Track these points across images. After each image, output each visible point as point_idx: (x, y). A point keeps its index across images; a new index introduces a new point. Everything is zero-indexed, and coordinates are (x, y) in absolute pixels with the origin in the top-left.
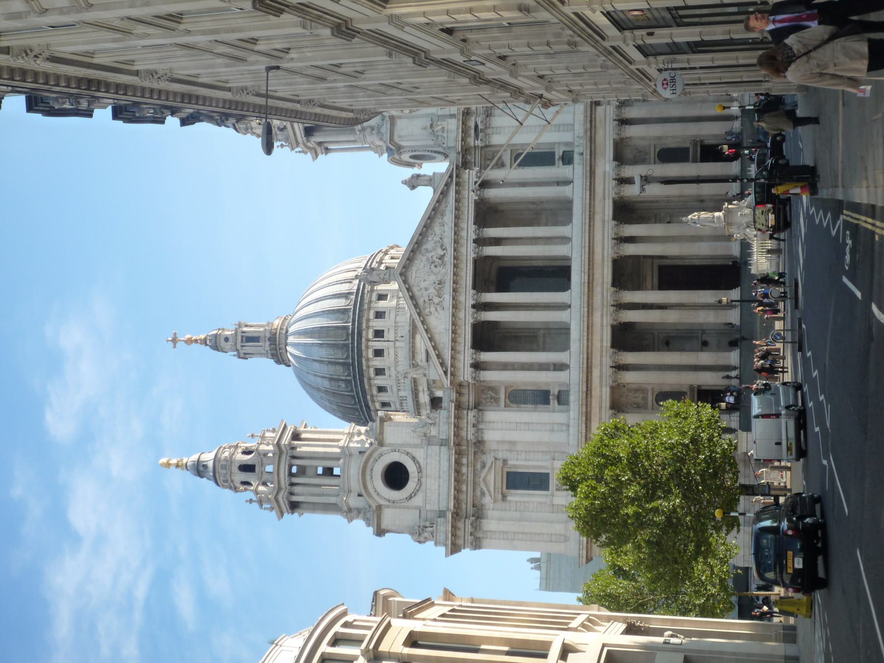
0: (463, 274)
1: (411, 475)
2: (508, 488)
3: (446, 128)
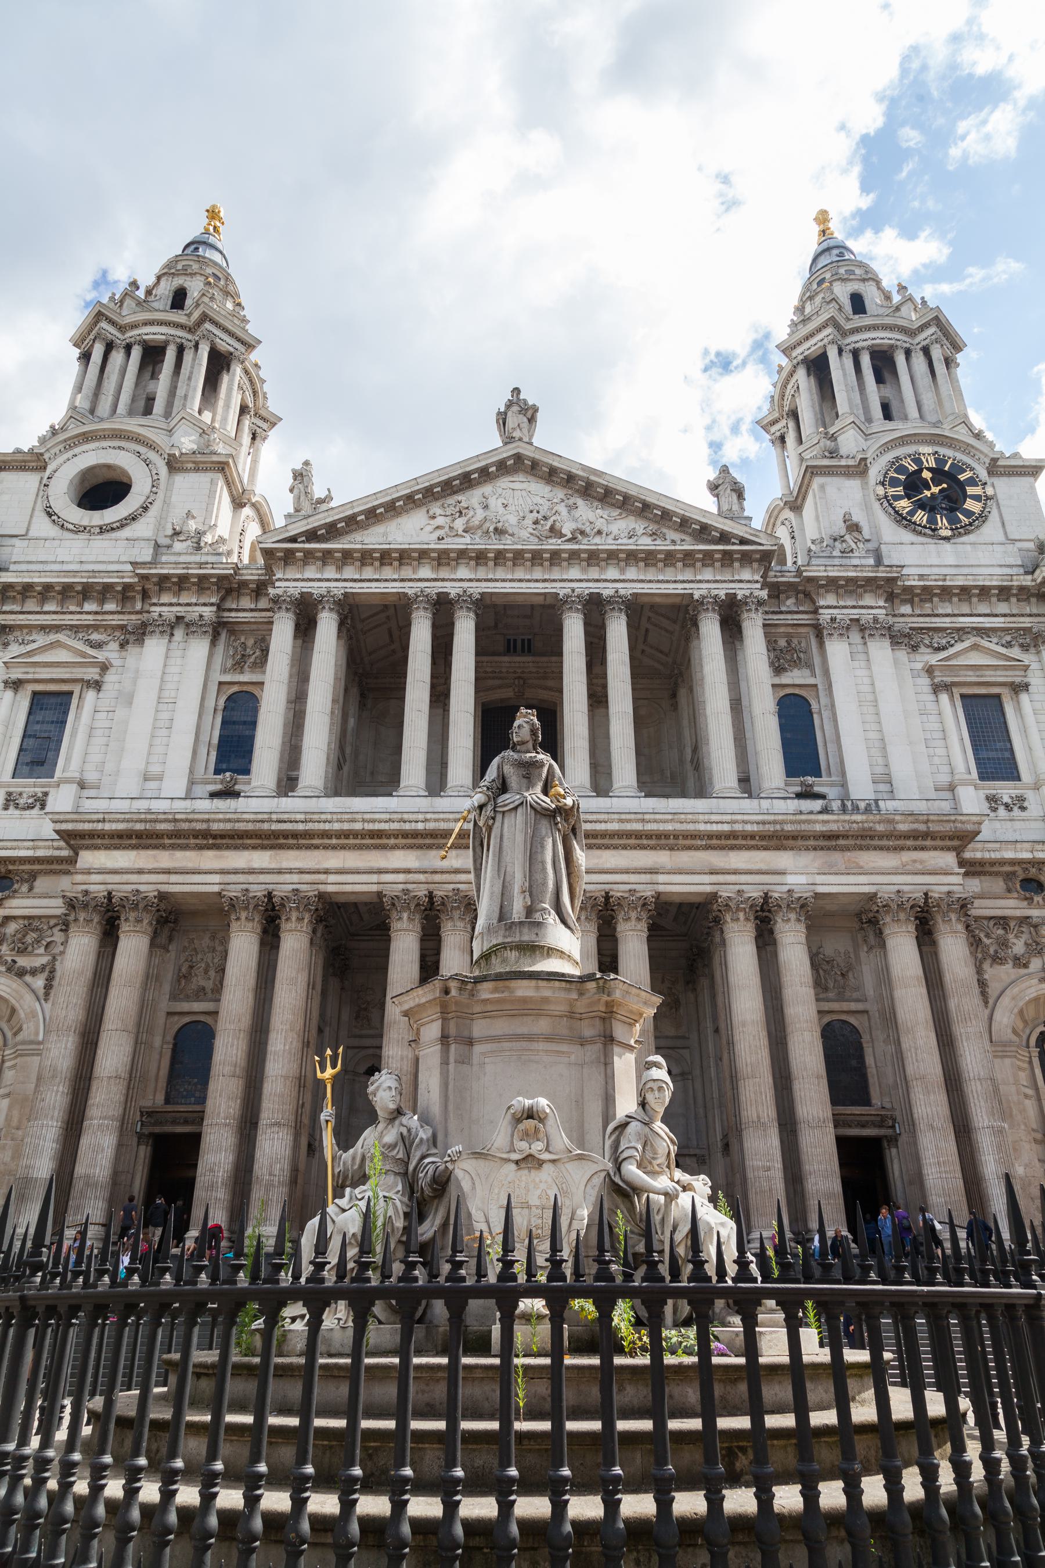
0: (520, 574)
1: (96, 514)
2: (35, 694)
3: (851, 555)
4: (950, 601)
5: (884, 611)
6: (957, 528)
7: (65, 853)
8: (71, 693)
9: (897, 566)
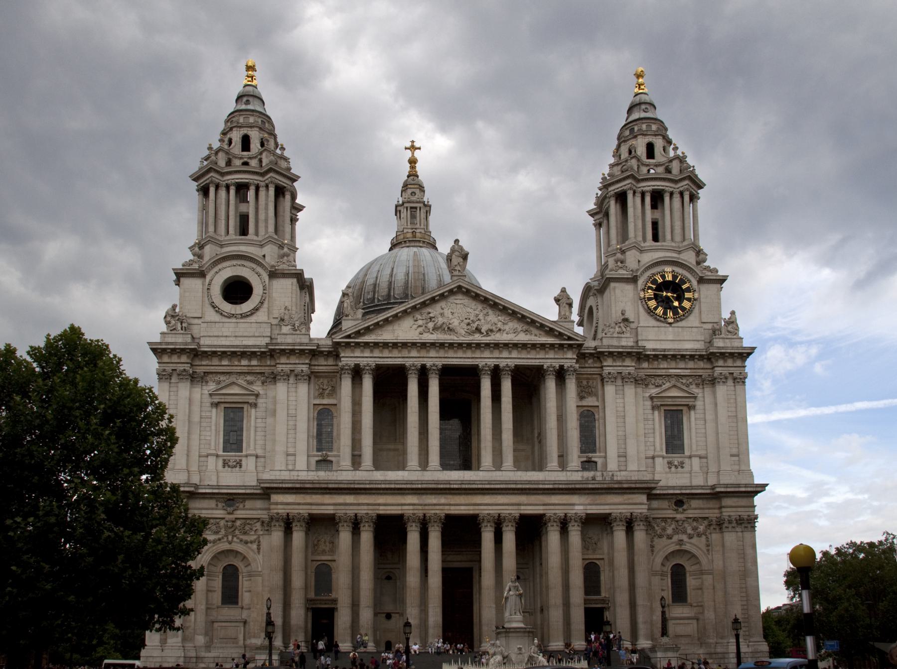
0: (460, 354)
2: (225, 408)
3: (623, 336)
4: (666, 360)
5: (634, 368)
7: (258, 491)
8: (243, 408)
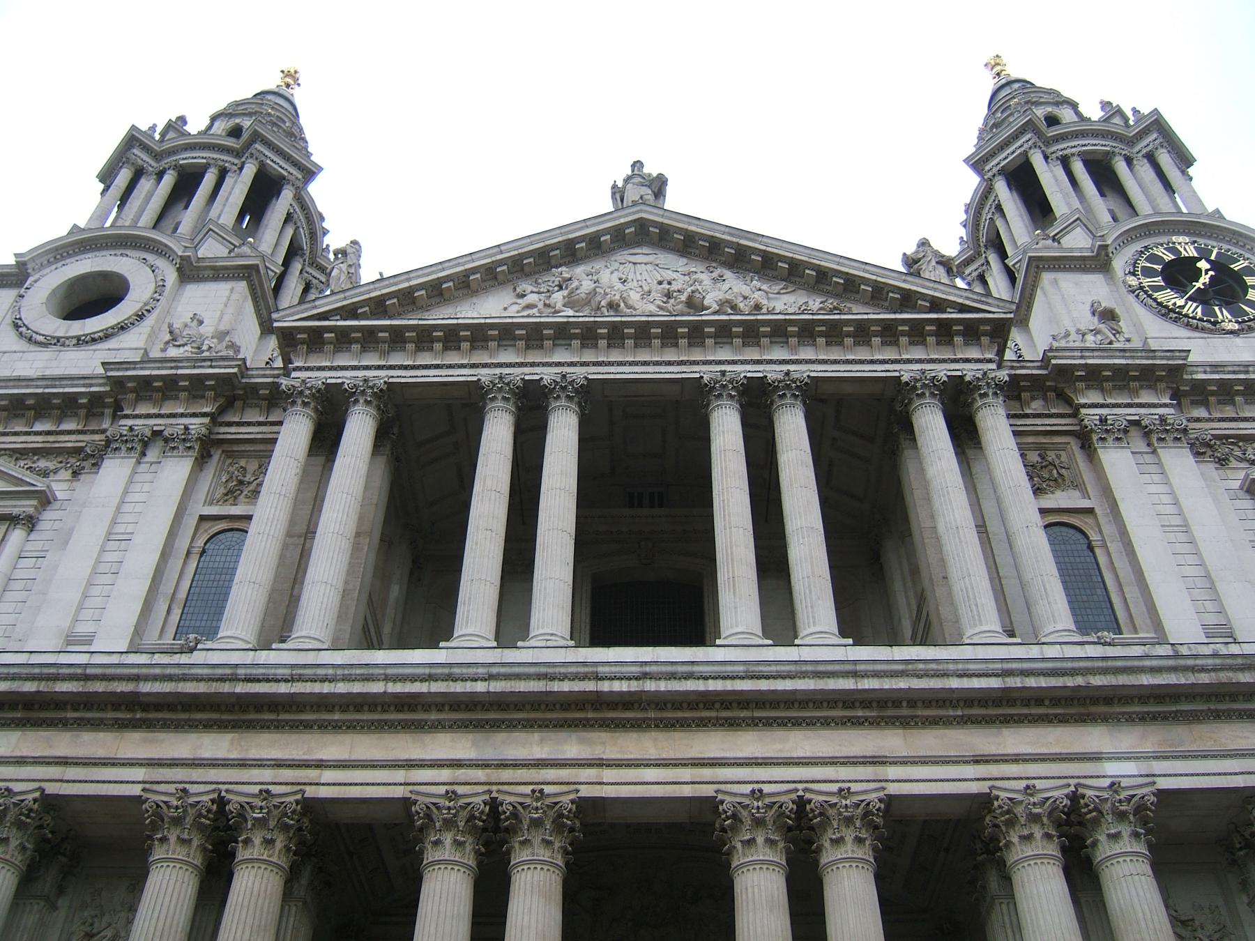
5: (1172, 411)
6: (1244, 321)
9: (1180, 351)
